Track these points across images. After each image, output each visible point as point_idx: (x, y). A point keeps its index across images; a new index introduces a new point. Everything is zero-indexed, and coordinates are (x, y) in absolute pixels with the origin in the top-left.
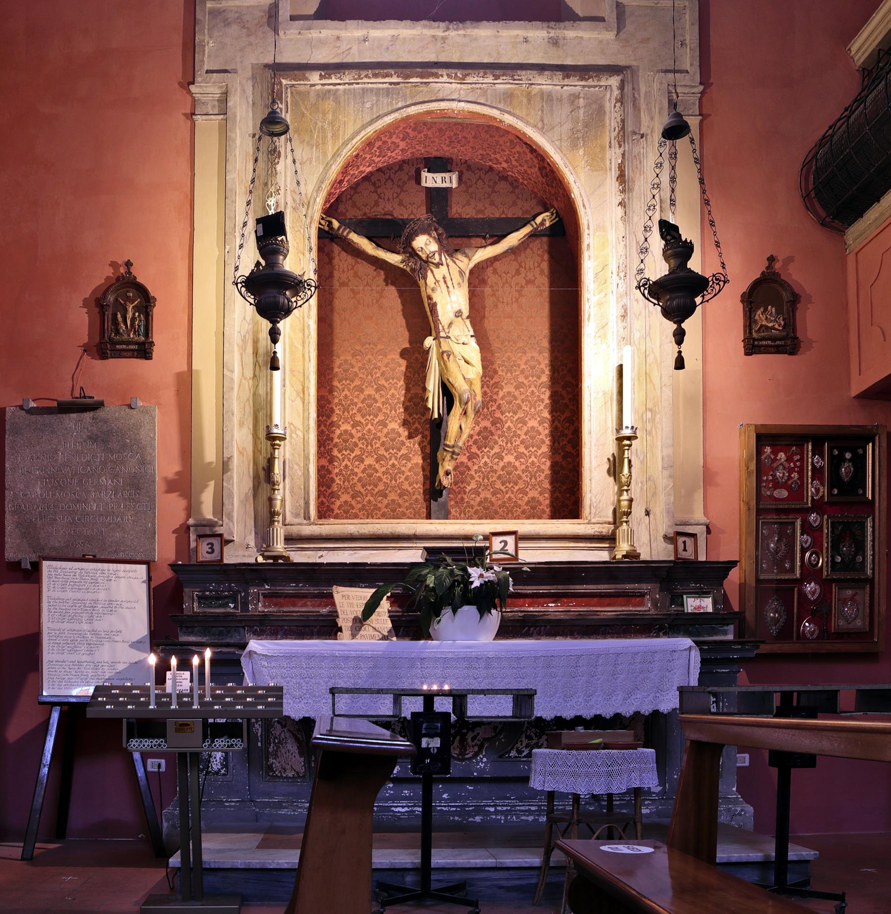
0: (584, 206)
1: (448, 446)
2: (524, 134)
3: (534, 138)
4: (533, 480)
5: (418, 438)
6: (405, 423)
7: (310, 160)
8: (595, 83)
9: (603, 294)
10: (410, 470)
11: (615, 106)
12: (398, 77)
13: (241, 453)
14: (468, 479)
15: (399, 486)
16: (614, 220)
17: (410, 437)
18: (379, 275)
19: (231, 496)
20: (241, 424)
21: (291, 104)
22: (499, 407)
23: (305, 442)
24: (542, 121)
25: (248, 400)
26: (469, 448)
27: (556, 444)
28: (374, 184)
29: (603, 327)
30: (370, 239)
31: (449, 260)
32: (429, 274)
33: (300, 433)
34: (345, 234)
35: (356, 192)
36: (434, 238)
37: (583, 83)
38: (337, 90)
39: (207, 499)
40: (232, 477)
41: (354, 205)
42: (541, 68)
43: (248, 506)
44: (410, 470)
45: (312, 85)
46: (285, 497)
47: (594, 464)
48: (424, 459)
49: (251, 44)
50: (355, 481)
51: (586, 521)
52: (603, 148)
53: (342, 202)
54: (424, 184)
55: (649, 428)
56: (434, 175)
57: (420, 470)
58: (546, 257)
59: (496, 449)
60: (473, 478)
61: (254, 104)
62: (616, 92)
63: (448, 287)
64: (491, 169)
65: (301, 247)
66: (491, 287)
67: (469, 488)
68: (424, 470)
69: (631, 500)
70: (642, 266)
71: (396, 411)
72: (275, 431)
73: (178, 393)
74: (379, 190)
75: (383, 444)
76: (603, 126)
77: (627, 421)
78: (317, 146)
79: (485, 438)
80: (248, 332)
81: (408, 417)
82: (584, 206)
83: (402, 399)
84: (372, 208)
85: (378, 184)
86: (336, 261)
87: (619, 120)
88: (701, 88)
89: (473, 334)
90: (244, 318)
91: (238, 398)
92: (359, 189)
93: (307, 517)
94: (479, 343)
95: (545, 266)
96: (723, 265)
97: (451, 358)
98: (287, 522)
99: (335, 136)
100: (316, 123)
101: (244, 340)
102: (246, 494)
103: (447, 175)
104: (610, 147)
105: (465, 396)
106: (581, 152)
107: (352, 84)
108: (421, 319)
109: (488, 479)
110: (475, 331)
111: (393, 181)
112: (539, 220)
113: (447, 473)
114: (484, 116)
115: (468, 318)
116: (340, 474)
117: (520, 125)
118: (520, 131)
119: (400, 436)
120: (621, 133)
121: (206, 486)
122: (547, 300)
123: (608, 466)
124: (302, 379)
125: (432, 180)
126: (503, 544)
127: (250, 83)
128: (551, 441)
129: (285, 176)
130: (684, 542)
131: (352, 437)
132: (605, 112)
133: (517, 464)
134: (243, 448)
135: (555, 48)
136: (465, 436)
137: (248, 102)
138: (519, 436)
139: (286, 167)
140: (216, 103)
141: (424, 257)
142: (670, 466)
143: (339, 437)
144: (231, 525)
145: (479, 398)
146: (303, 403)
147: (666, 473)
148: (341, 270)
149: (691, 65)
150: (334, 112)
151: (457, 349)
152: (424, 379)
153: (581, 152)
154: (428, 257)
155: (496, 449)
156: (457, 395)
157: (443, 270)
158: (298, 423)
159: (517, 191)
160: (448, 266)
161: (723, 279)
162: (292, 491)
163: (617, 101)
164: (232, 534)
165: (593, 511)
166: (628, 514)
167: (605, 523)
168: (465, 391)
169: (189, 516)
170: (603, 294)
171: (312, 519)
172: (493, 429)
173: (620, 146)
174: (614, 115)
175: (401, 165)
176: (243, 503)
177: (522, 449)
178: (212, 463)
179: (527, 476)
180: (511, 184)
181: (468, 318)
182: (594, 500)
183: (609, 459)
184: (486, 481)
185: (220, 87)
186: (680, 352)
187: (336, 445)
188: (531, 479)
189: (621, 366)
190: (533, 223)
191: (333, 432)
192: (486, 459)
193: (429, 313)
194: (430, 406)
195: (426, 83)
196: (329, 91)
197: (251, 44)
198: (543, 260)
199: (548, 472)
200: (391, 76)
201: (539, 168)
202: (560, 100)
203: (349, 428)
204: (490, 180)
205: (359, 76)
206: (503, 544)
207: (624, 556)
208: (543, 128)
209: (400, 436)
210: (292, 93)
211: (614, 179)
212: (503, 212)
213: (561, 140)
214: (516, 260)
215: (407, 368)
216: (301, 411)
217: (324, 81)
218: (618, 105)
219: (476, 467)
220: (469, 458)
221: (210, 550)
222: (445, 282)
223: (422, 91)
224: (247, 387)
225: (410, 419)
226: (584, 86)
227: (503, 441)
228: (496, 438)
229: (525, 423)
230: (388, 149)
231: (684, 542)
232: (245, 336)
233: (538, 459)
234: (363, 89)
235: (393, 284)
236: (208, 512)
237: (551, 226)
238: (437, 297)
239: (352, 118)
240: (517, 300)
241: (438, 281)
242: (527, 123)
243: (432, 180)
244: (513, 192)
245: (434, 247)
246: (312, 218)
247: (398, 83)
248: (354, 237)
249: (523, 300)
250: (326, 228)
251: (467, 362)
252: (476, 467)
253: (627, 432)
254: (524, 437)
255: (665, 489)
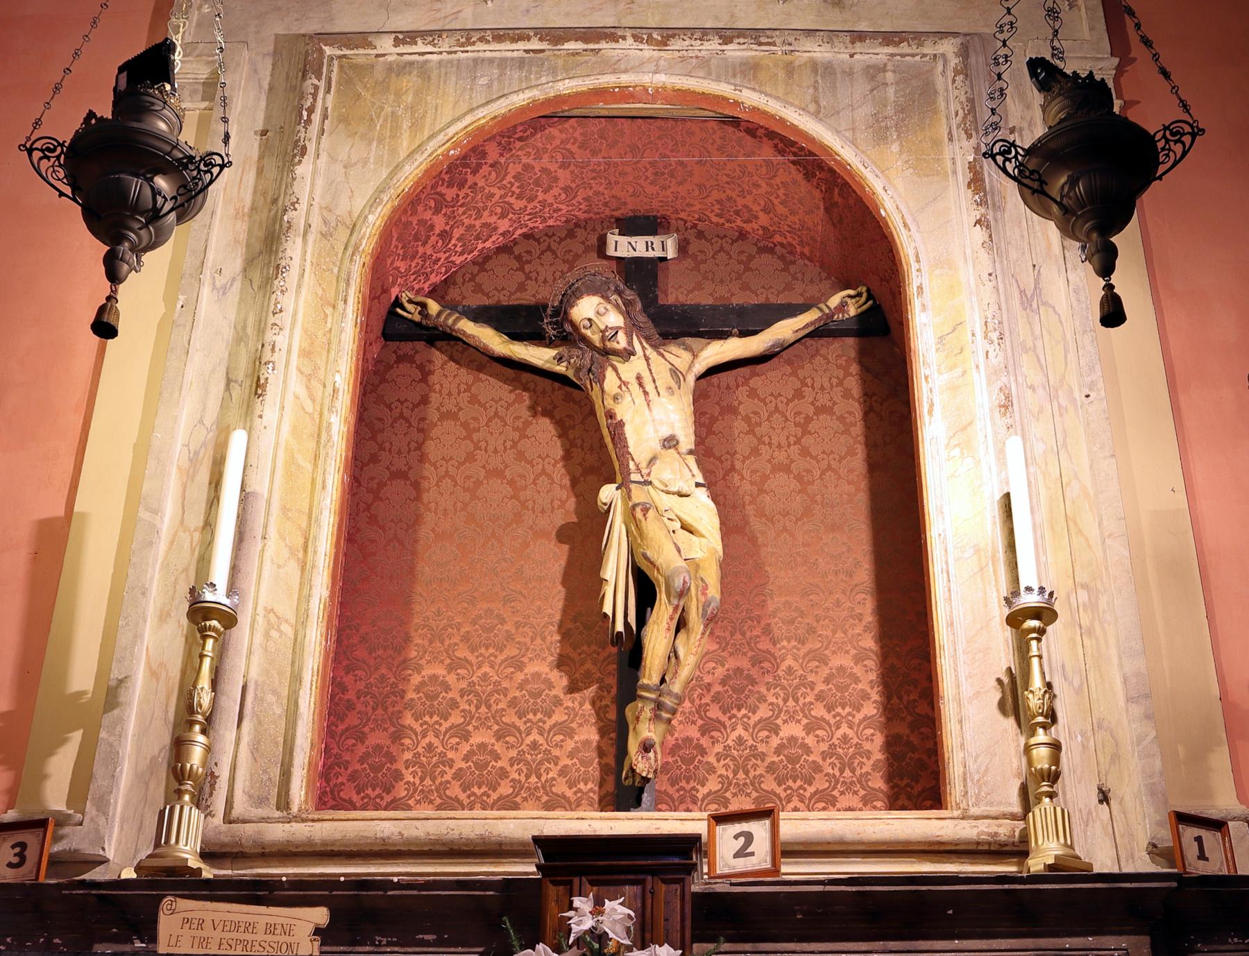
0: (905, 225)
1: (647, 688)
2: (782, 121)
3: (801, 127)
4: (847, 773)
5: (591, 691)
6: (562, 663)
7: (365, 162)
8: (914, 50)
9: (958, 371)
10: (571, 755)
11: (954, 81)
12: (541, 40)
13: (153, 674)
14: (702, 772)
15: (547, 786)
16: (969, 251)
17: (572, 689)
18: (519, 400)
19: (113, 760)
20: (163, 617)
21: (339, 83)
22: (767, 630)
23: (297, 645)
24: (817, 102)
25: (186, 570)
26: (701, 710)
27: (895, 700)
28: (518, 258)
29: (964, 429)
30: (499, 328)
31: (650, 352)
32: (610, 373)
33: (288, 630)
34: (450, 321)
35: (482, 269)
36: (617, 306)
37: (891, 50)
38: (427, 61)
39: (61, 767)
40: (121, 721)
41: (478, 289)
42: (810, 32)
43: (152, 786)
44: (571, 755)
45: (377, 56)
46: (233, 756)
47: (967, 690)
48: (602, 732)
49: (279, 9)
50: (448, 777)
51: (956, 813)
52: (936, 143)
53: (455, 283)
54: (611, 252)
55: (1085, 621)
56: (633, 240)
57: (592, 754)
58: (854, 368)
59: (763, 712)
60: (712, 770)
61: (271, 88)
62: (954, 61)
63: (646, 393)
64: (742, 235)
65: (331, 295)
66: (747, 419)
67: (703, 791)
68: (601, 753)
69: (1056, 747)
70: (996, 118)
71: (544, 639)
72: (208, 596)
73: (36, 556)
74: (527, 268)
75: (513, 703)
76: (935, 111)
77: (1028, 576)
78: (380, 141)
79: (738, 690)
80: (204, 444)
81: (569, 650)
82: (905, 225)
83: (558, 617)
84: (511, 294)
85: (526, 257)
86: (434, 379)
87: (963, 99)
88: (1116, 61)
89: (701, 480)
90: (201, 422)
91: (165, 566)
92: (487, 266)
93: (283, 802)
94: (714, 499)
95: (853, 384)
96: (1185, 107)
97: (651, 513)
98: (235, 813)
99: (416, 126)
100: (382, 109)
101: (194, 460)
102: (153, 758)
103: (656, 240)
104: (951, 140)
105: (678, 583)
106: (895, 147)
107: (455, 52)
108: (594, 453)
109: (747, 773)
110: (705, 478)
111: (554, 252)
112: (834, 301)
113: (646, 747)
114: (704, 96)
115: (691, 452)
116: (415, 761)
117: (773, 106)
118: (772, 117)
119: (551, 686)
120: (970, 118)
121: (63, 741)
122: (861, 439)
123: (998, 696)
124: (304, 525)
125: (623, 246)
126: (742, 840)
127: (269, 62)
128: (882, 694)
129: (313, 184)
130: (1199, 840)
131: (447, 688)
132: (936, 92)
133: (810, 741)
134: (161, 665)
135: (837, 10)
136: (685, 672)
137: (260, 87)
138: (812, 686)
139: (315, 171)
140: (201, 88)
141: (596, 338)
142: (1142, 694)
143: (417, 690)
144: (102, 821)
145: (714, 592)
146: (303, 569)
147: (1137, 710)
148: (445, 391)
149: (1092, 29)
150: (416, 94)
151: (665, 501)
152: (598, 558)
153: (895, 147)
154: (603, 339)
155: (763, 712)
156: (661, 580)
157: (636, 365)
158: (287, 610)
159: (792, 269)
160: (647, 359)
161: (1187, 129)
162: (255, 749)
163: (957, 72)
164: (100, 841)
165: (972, 790)
166: (1053, 777)
167: (1004, 816)
168: (677, 571)
169: (10, 806)
170: (958, 371)
171: (295, 809)
172: (754, 672)
173: (969, 136)
174: (953, 93)
175: (573, 228)
176: (141, 779)
177: (819, 711)
178: (84, 693)
179: (833, 765)
180: (782, 258)
181: (691, 452)
182: (972, 766)
183: (999, 681)
184: (741, 775)
185: (208, 63)
186: (1109, 287)
187: (410, 705)
188: (842, 771)
189: (1008, 495)
190: (822, 306)
191: (406, 680)
192: (740, 731)
193: (608, 440)
194: (607, 609)
195: (592, 50)
196: (411, 63)
197: (279, 9)
198: (847, 374)
199: (878, 756)
200: (529, 39)
201: (826, 209)
202: (850, 73)
203: (440, 671)
204: (742, 252)
205: (468, 39)
206: (742, 840)
207: (1050, 867)
208: (819, 112)
209: (551, 686)
210: (341, 67)
211: (963, 187)
212: (767, 298)
213: (853, 129)
214: (794, 374)
215: (570, 564)
216: (297, 587)
217: (399, 50)
218: (960, 78)
219: (719, 748)
220: (704, 731)
221: (15, 860)
222: (641, 385)
223: (586, 62)
224: (187, 546)
225: (574, 655)
226: (892, 55)
227: (777, 696)
228: (763, 690)
229: (824, 661)
230: (537, 183)
231: (1199, 840)
232: (197, 453)
233: (862, 729)
234: (475, 60)
235: (546, 413)
236: (55, 798)
237: (859, 316)
238: (623, 411)
239: (451, 99)
240: (798, 442)
241: (626, 384)
242: (787, 103)
243: (623, 246)
244: (785, 270)
245: (614, 319)
246: (356, 248)
247: (542, 51)
248: (468, 327)
249: (808, 441)
250: (417, 318)
251: (685, 527)
252: (719, 748)
253: (1030, 600)
254: (824, 687)
255: (1139, 742)
